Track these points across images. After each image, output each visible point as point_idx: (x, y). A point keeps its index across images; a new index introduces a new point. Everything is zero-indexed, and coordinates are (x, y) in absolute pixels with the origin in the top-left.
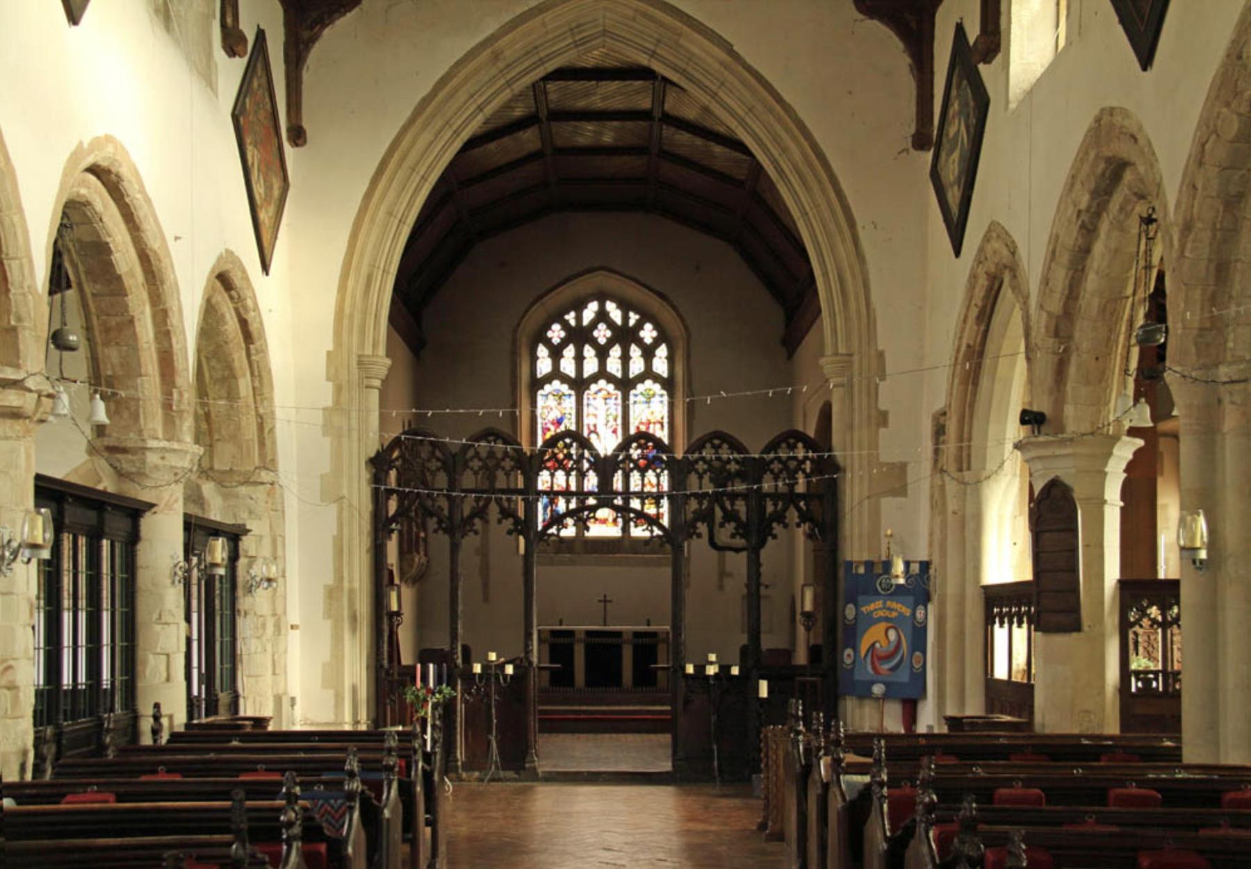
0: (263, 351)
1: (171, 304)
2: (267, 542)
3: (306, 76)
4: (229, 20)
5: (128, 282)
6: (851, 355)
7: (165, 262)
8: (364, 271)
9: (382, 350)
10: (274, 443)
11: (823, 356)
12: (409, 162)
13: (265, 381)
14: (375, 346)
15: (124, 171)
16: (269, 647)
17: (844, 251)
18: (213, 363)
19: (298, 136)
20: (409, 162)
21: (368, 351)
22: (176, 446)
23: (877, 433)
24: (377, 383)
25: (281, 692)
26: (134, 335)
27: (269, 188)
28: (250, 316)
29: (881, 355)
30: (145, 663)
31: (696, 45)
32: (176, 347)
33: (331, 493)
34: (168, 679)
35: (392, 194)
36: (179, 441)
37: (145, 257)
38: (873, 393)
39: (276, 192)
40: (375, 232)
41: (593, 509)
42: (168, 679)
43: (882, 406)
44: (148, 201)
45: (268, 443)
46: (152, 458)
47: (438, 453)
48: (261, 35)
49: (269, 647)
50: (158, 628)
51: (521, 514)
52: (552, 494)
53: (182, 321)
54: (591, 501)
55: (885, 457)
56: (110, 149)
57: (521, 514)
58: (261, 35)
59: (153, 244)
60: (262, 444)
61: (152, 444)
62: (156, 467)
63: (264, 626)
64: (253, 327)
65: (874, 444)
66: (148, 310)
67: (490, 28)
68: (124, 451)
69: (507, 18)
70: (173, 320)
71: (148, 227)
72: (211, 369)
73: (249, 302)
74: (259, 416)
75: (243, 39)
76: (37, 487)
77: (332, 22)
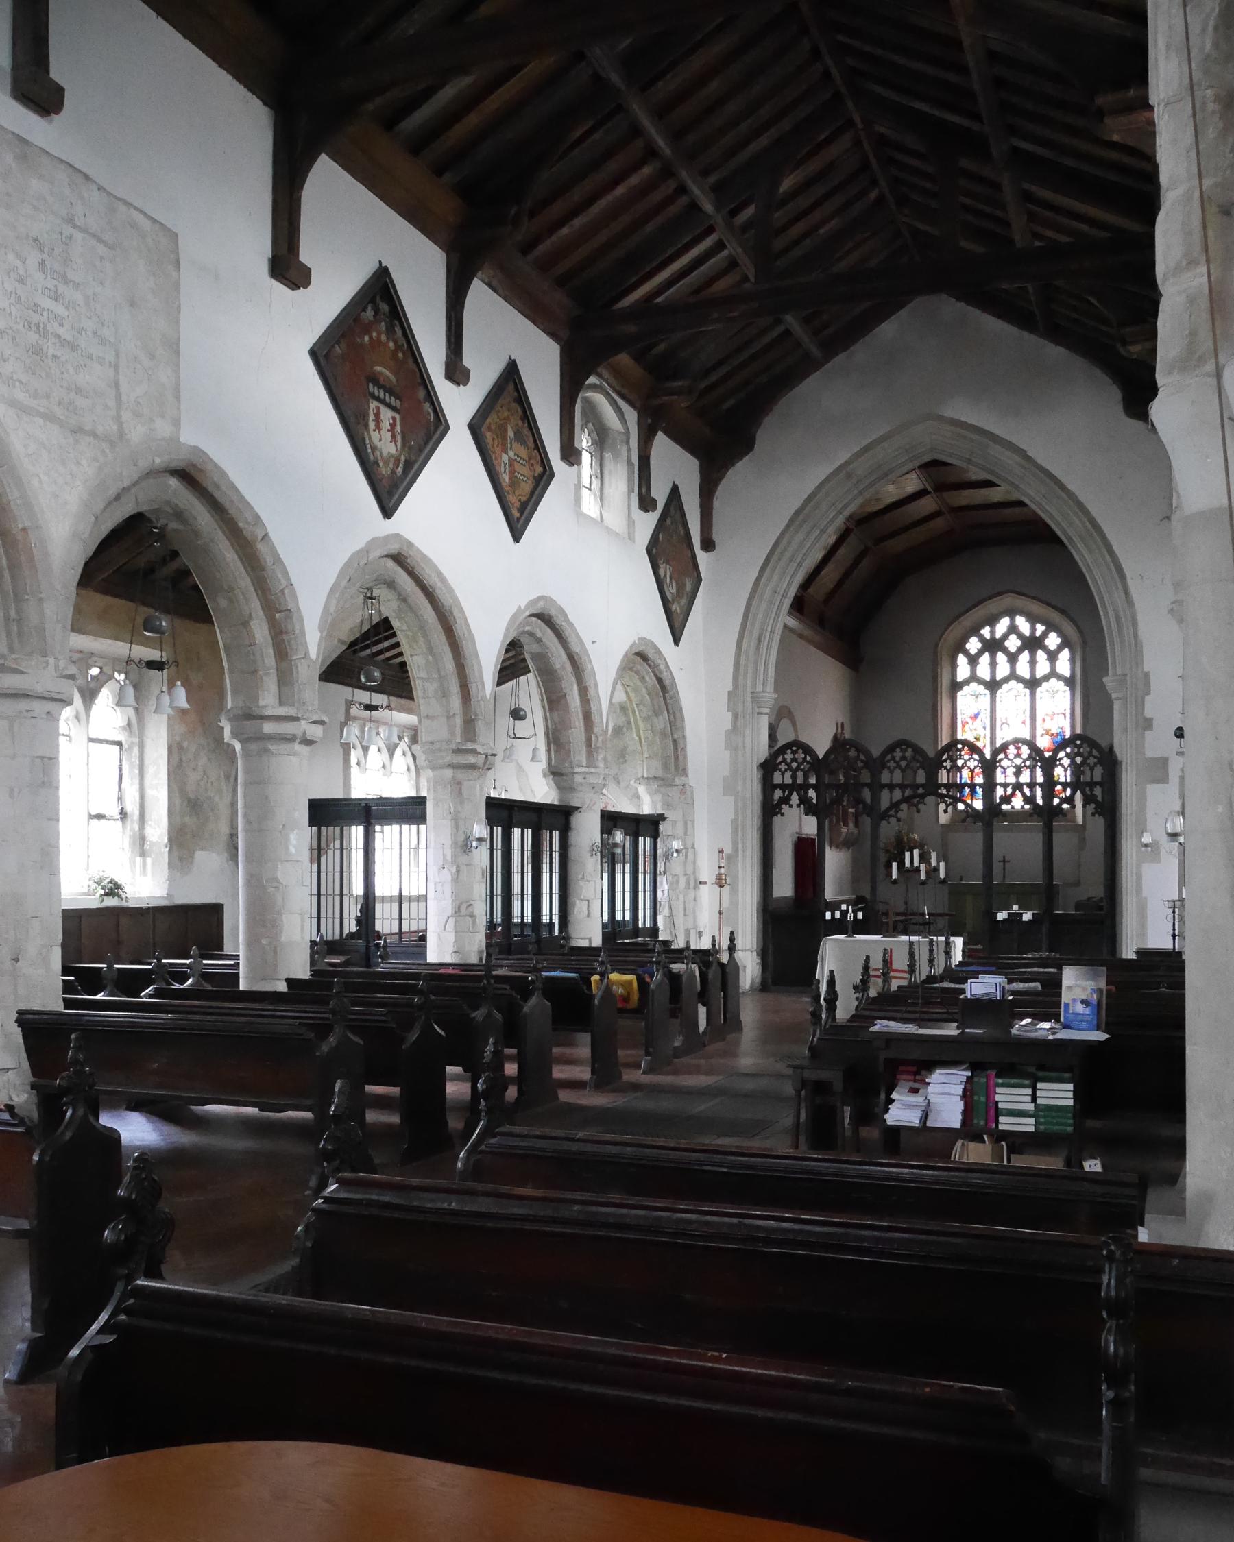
0: (676, 698)
1: (590, 683)
2: (680, 825)
3: (716, 504)
4: (644, 491)
5: (561, 673)
6: (1125, 675)
7: (584, 658)
8: (756, 632)
9: (770, 688)
10: (685, 757)
11: (1107, 675)
12: (788, 555)
13: (678, 715)
14: (765, 684)
15: (553, 612)
16: (681, 896)
17: (1119, 596)
18: (641, 707)
19: (708, 545)
20: (788, 555)
21: (759, 688)
22: (593, 770)
23: (1143, 737)
24: (767, 710)
25: (690, 926)
26: (567, 705)
27: (681, 587)
28: (664, 676)
29: (1147, 675)
30: (574, 906)
31: (995, 450)
32: (593, 708)
33: (729, 787)
34: (588, 916)
35: (775, 577)
36: (596, 767)
37: (572, 658)
38: (1140, 705)
39: (689, 587)
40: (764, 606)
41: (923, 796)
42: (588, 916)
43: (1148, 714)
44: (571, 625)
45: (681, 758)
46: (578, 779)
47: (808, 758)
48: (675, 490)
49: (681, 896)
50: (581, 883)
51: (868, 800)
52: (891, 787)
53: (597, 692)
54: (921, 791)
55: (1149, 754)
56: (541, 604)
57: (868, 800)
58: (675, 490)
59: (575, 648)
60: (677, 758)
61: (578, 770)
62: (581, 784)
63: (678, 882)
64: (667, 682)
65: (1140, 747)
66: (575, 687)
67: (844, 456)
68: (562, 775)
69: (865, 442)
70: (591, 692)
71: (572, 641)
72: (640, 711)
73: (662, 667)
74: (675, 742)
75: (654, 502)
76: (487, 804)
77: (733, 465)
